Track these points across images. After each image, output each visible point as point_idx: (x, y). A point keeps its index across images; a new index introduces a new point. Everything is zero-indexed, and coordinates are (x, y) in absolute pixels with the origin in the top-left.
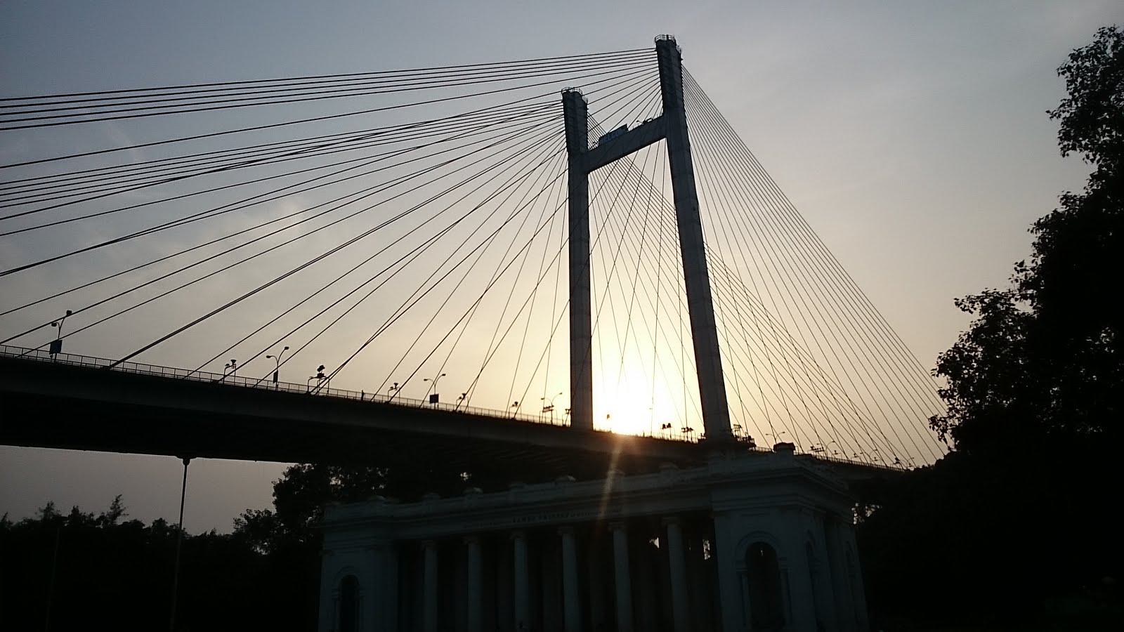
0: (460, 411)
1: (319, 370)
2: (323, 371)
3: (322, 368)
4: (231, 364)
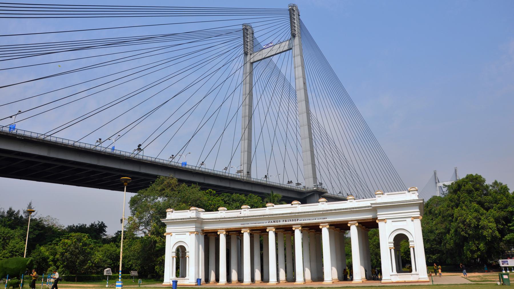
1: (139, 146)
2: (141, 147)
3: (140, 145)
4: (99, 141)
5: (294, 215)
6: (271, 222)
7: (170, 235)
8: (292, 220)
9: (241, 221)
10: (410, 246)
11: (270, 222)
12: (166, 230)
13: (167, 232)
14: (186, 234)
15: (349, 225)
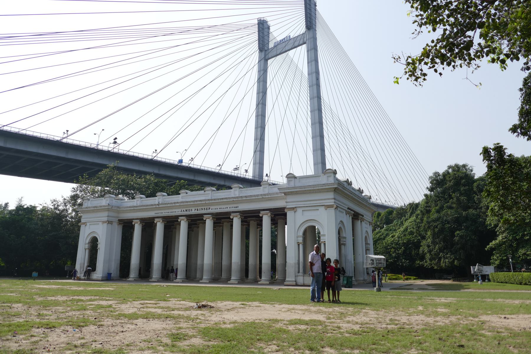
0: (190, 167)
1: (114, 139)
2: (116, 140)
3: (116, 138)
5: (204, 202)
6: (184, 211)
7: (84, 225)
8: (203, 209)
9: (155, 210)
10: (321, 241)
11: (182, 211)
12: (82, 220)
13: (82, 222)
14: (99, 224)
15: (261, 215)
